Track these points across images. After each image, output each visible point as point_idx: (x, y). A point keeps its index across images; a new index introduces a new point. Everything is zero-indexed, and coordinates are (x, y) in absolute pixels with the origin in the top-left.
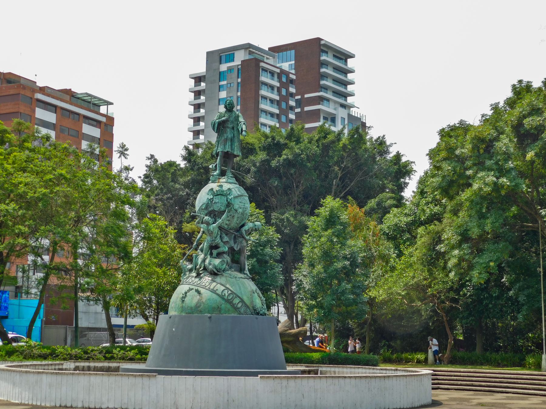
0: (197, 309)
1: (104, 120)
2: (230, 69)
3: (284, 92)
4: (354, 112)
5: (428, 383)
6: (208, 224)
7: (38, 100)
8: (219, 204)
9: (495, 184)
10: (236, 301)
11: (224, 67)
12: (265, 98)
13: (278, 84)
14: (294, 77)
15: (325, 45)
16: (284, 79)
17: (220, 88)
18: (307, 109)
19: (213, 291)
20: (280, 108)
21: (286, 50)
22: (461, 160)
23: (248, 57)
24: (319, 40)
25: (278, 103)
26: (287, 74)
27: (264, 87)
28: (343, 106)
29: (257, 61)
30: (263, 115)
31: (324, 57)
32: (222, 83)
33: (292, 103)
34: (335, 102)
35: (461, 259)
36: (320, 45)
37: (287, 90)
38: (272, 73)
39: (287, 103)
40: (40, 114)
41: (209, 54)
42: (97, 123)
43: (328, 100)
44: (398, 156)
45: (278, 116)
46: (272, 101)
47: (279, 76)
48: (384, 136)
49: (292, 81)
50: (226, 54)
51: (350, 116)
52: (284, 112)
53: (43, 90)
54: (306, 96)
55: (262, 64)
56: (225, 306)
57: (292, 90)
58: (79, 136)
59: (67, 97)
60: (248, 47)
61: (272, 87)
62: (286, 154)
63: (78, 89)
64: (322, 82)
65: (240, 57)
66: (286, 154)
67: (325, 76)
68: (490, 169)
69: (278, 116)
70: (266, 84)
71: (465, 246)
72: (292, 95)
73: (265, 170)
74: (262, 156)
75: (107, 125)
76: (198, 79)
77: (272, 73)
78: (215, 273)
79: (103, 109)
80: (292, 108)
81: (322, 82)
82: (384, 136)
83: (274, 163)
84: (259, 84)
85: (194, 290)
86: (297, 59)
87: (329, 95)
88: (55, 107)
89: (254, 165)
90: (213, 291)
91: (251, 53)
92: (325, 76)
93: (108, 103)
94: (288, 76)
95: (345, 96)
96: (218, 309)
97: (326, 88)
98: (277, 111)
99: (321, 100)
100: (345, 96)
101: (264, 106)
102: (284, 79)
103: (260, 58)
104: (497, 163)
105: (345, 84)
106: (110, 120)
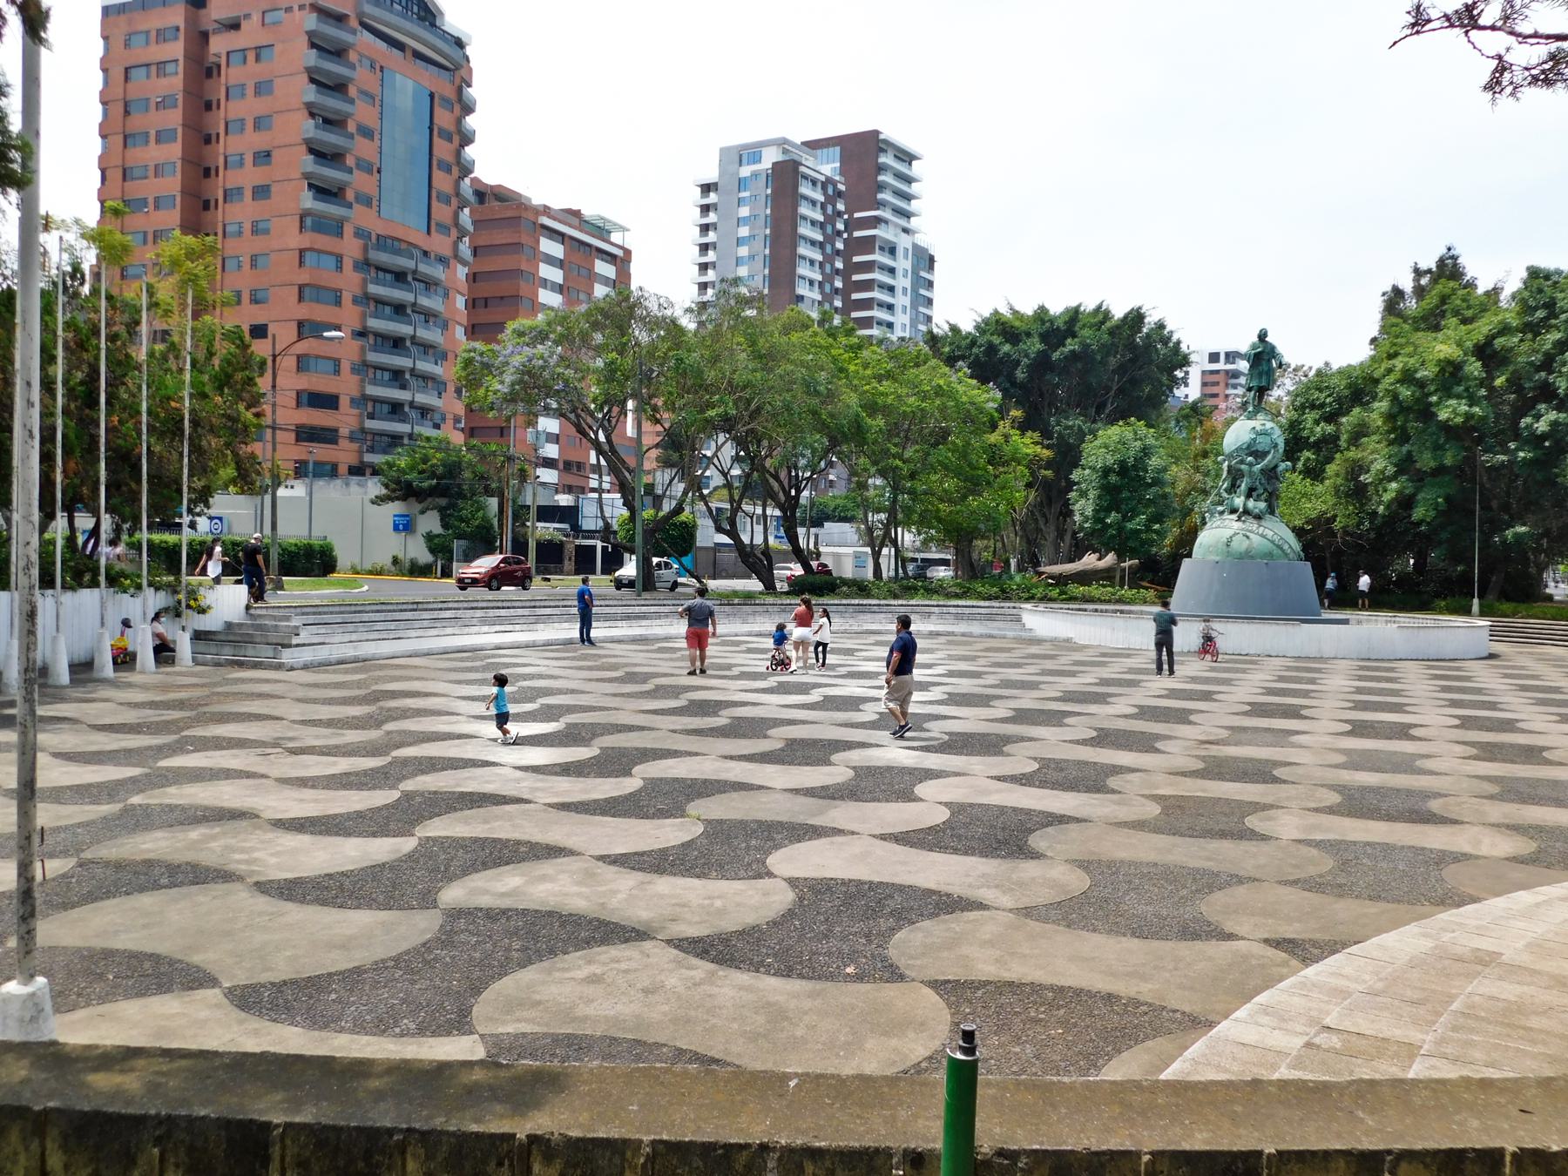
0: (1247, 555)
1: (620, 253)
2: (755, 175)
3: (829, 209)
4: (921, 240)
5: (1486, 633)
6: (1251, 465)
7: (544, 227)
8: (1263, 444)
9: (1466, 413)
10: (1286, 547)
11: (746, 171)
12: (804, 218)
13: (822, 199)
14: (842, 187)
15: (885, 142)
16: (830, 191)
17: (740, 202)
18: (857, 234)
19: (1263, 536)
20: (824, 234)
21: (828, 146)
22: (1421, 384)
23: (780, 158)
24: (876, 133)
25: (822, 226)
26: (834, 184)
27: (804, 203)
28: (906, 231)
29: (796, 164)
30: (802, 243)
31: (883, 159)
32: (742, 195)
33: (840, 226)
34: (896, 225)
35: (1399, 492)
36: (878, 141)
37: (834, 206)
38: (814, 182)
39: (834, 226)
40: (549, 246)
41: (722, 150)
42: (611, 258)
43: (886, 222)
44: (1178, 343)
45: (822, 245)
46: (813, 223)
47: (824, 186)
48: (1262, 336)
49: (839, 194)
50: (747, 153)
51: (915, 246)
52: (830, 239)
53: (546, 211)
54: (857, 215)
55: (802, 169)
56: (1276, 551)
57: (841, 207)
58: (593, 277)
59: (576, 221)
60: (783, 143)
61: (814, 203)
62: (1071, 345)
63: (588, 212)
64: (880, 196)
65: (770, 157)
66: (1071, 345)
67: (881, 187)
68: (1459, 397)
69: (822, 245)
70: (806, 198)
71: (1404, 478)
72: (839, 214)
73: (1042, 364)
74: (1035, 346)
75: (622, 261)
76: (707, 188)
77: (814, 182)
78: (1258, 517)
79: (616, 237)
80: (839, 233)
81: (880, 196)
82: (1262, 336)
83: (1056, 356)
84: (797, 198)
85: (1220, 533)
86: (844, 160)
87: (886, 214)
88: (562, 235)
89: (1027, 356)
90: (1263, 536)
91: (785, 151)
92: (881, 187)
93: (624, 229)
94: (835, 186)
95: (907, 215)
96: (1270, 555)
97: (880, 204)
98: (821, 238)
99: (876, 222)
100: (907, 215)
101: (805, 230)
102: (830, 191)
103: (796, 158)
104: (1467, 390)
105: (908, 197)
106: (628, 252)
